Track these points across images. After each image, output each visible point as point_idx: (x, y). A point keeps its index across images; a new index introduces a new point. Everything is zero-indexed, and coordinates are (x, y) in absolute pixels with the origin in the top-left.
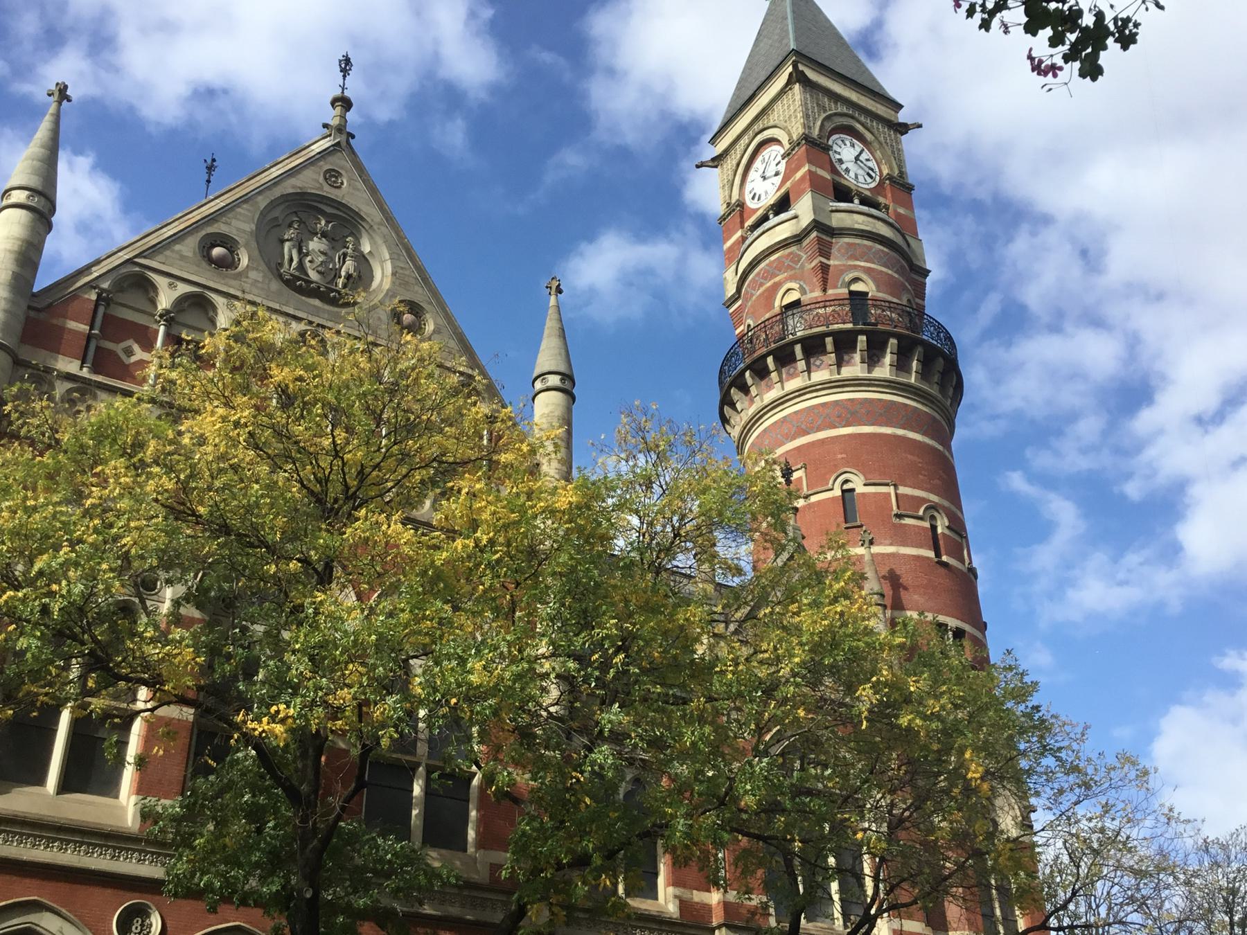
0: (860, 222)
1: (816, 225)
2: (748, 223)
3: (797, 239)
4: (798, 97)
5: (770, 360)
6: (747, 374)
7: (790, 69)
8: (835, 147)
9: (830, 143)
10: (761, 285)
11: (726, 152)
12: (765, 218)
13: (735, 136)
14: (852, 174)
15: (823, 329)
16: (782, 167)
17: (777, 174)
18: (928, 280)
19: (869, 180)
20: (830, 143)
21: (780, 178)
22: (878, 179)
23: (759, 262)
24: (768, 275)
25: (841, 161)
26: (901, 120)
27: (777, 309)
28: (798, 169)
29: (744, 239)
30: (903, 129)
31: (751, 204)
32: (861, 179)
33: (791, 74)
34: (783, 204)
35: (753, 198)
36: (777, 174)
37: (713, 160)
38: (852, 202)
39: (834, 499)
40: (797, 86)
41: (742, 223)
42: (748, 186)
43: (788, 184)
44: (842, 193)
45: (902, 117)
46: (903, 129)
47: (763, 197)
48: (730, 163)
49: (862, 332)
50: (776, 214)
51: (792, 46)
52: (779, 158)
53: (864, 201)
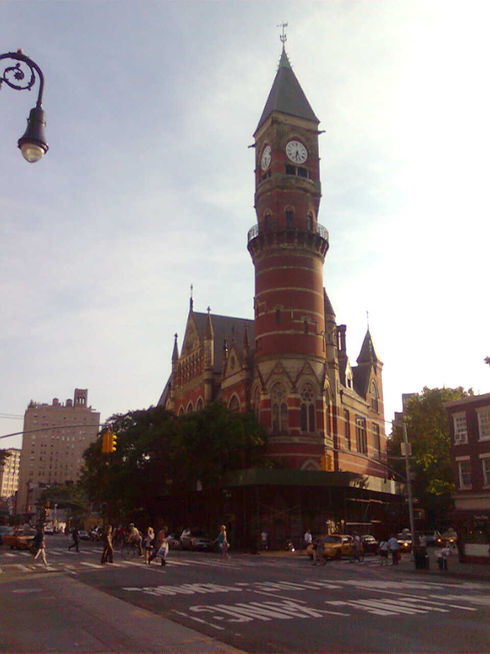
45: (320, 128)
46: (320, 133)
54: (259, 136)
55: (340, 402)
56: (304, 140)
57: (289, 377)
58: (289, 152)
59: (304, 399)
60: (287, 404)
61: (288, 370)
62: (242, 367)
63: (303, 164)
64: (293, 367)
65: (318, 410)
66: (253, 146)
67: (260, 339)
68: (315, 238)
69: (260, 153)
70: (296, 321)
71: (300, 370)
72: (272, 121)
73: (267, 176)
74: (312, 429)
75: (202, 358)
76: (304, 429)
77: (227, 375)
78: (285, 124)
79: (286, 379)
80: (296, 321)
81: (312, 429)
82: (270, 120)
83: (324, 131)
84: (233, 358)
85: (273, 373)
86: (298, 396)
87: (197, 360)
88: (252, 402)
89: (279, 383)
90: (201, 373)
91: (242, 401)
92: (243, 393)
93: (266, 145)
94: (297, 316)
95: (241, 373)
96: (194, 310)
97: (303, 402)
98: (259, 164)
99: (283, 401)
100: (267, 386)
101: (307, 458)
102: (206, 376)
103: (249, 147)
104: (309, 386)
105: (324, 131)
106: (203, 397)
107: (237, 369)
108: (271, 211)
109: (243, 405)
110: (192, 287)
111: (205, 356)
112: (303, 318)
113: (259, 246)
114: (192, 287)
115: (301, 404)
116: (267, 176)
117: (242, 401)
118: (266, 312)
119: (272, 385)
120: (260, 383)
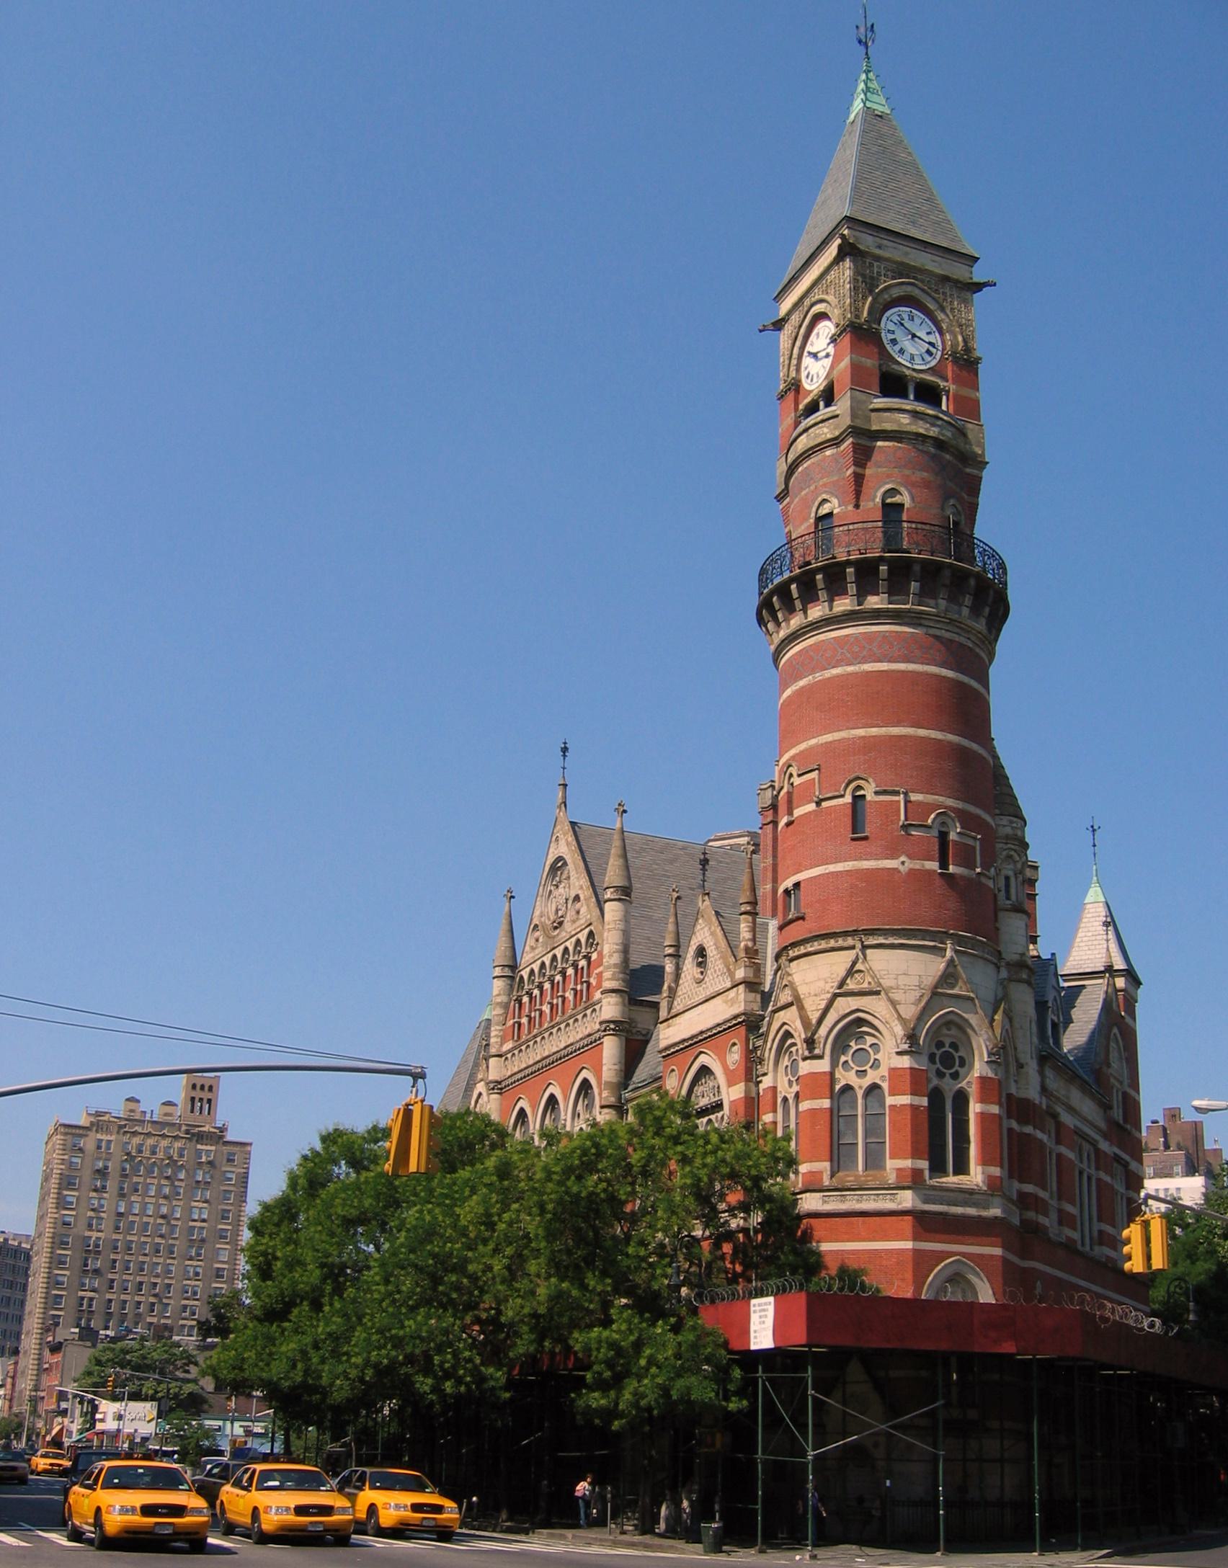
1: (854, 431)
3: (835, 442)
4: (847, 273)
11: (789, 313)
13: (822, 269)
17: (827, 356)
18: (985, 474)
19: (928, 358)
22: (938, 357)
23: (797, 467)
26: (975, 280)
31: (806, 385)
36: (827, 356)
37: (774, 324)
40: (847, 263)
48: (788, 329)
55: (1038, 1088)
56: (932, 306)
58: (892, 337)
59: (940, 1075)
60: (885, 1086)
61: (886, 983)
62: (731, 974)
63: (932, 370)
67: (797, 885)
68: (972, 582)
69: (798, 343)
72: (840, 247)
73: (822, 404)
75: (594, 956)
77: (678, 1007)
78: (878, 258)
82: (832, 250)
84: (701, 952)
85: (841, 991)
87: (575, 965)
88: (767, 1082)
89: (860, 1022)
90: (592, 1005)
91: (731, 1083)
92: (735, 1056)
93: (822, 316)
95: (732, 993)
97: (935, 1082)
98: (793, 374)
99: (872, 1077)
100: (823, 1031)
104: (954, 1031)
106: (598, 1075)
107: (717, 978)
108: (835, 501)
109: (733, 1094)
110: (565, 750)
111: (606, 951)
113: (798, 604)
114: (565, 750)
115: (931, 1086)
116: (822, 404)
117: (731, 1083)
118: (818, 804)
120: (798, 1024)
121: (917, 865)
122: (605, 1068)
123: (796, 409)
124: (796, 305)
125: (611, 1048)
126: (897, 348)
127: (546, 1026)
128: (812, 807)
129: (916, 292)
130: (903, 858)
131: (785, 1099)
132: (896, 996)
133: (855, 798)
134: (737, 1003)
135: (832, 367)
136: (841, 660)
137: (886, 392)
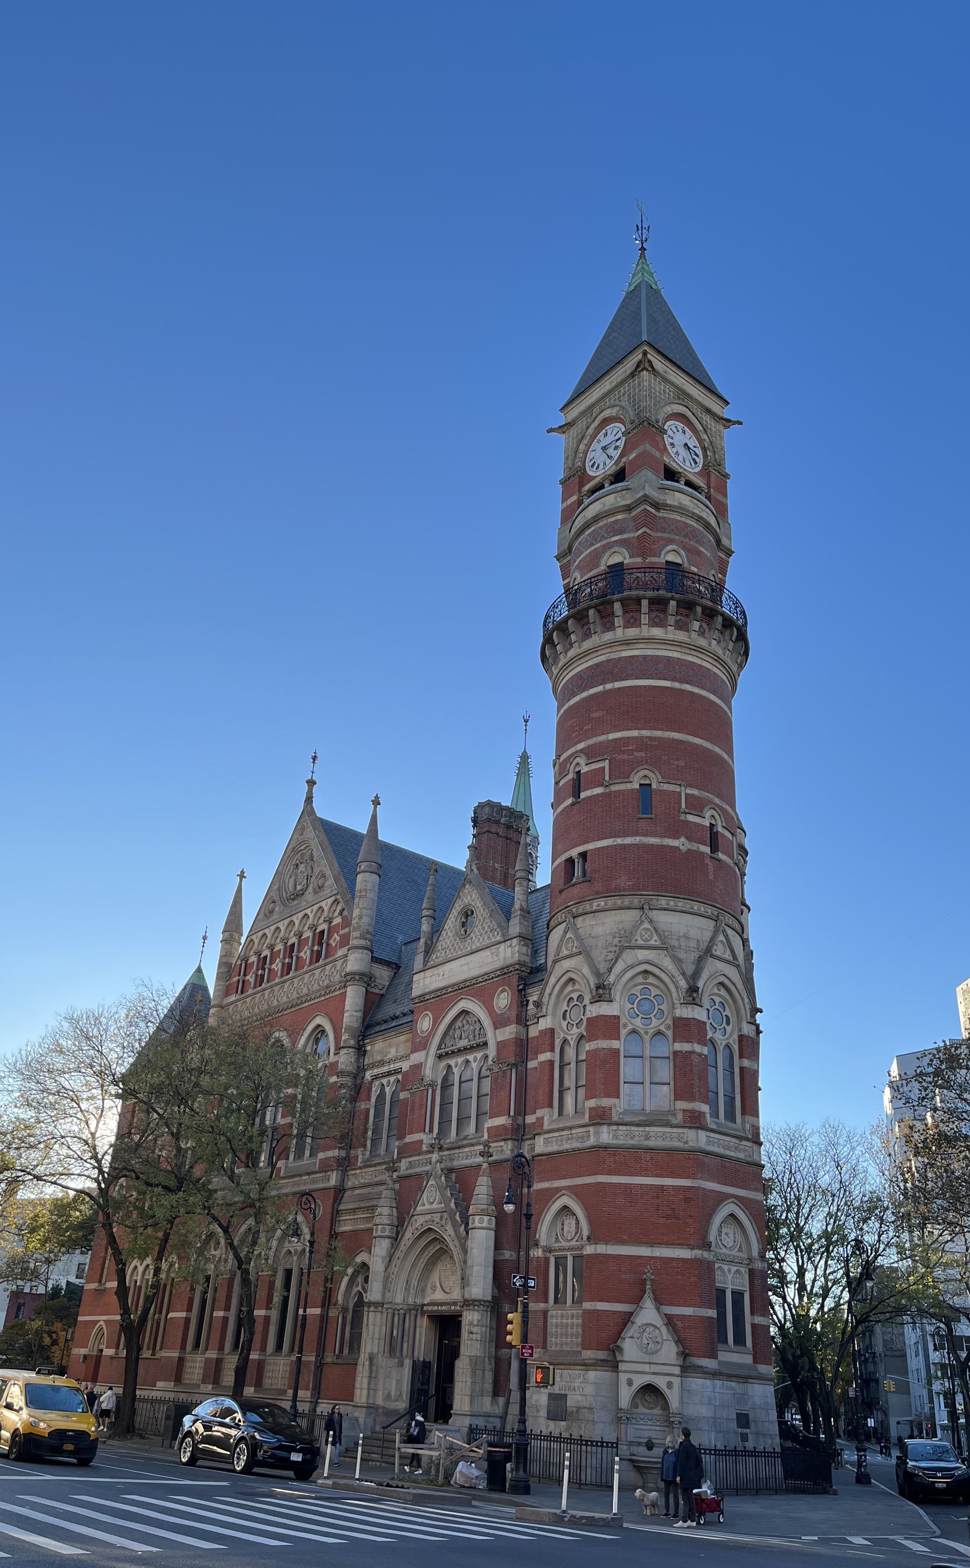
0: (685, 500)
2: (587, 488)
5: (591, 612)
6: (570, 622)
7: (638, 356)
8: (669, 432)
9: (666, 427)
10: (592, 545)
12: (601, 486)
14: (681, 458)
15: (642, 593)
16: (621, 443)
20: (666, 427)
21: (620, 451)
24: (595, 538)
25: (672, 444)
27: (602, 568)
28: (635, 446)
29: (580, 502)
30: (728, 422)
32: (687, 463)
33: (640, 362)
34: (619, 476)
35: (592, 466)
38: (678, 481)
39: (632, 790)
41: (581, 485)
42: (590, 455)
43: (624, 460)
44: (671, 474)
47: (601, 467)
48: (574, 432)
49: (672, 598)
50: (612, 484)
51: (644, 338)
52: (620, 435)
53: (689, 484)
54: (574, 413)
57: (678, 961)
58: (671, 441)
64: (687, 937)
65: (746, 1063)
66: (562, 429)
67: (583, 855)
69: (585, 441)
70: (691, 818)
71: (703, 946)
74: (731, 1116)
76: (715, 1114)
79: (667, 963)
80: (691, 818)
81: (731, 1116)
83: (740, 423)
86: (698, 1014)
94: (696, 806)
96: (322, 812)
101: (722, 1198)
102: (355, 961)
103: (550, 430)
104: (723, 992)
105: (740, 423)
110: (314, 758)
112: (708, 813)
114: (314, 758)
116: (606, 485)
119: (629, 974)
121: (695, 846)
122: (346, 1014)
123: (580, 491)
124: (583, 413)
125: (353, 998)
126: (675, 450)
127: (277, 980)
128: (599, 790)
129: (689, 414)
130: (683, 839)
131: (565, 1041)
132: (681, 955)
133: (641, 785)
134: (510, 953)
135: (621, 456)
136: (632, 675)
137: (667, 478)
